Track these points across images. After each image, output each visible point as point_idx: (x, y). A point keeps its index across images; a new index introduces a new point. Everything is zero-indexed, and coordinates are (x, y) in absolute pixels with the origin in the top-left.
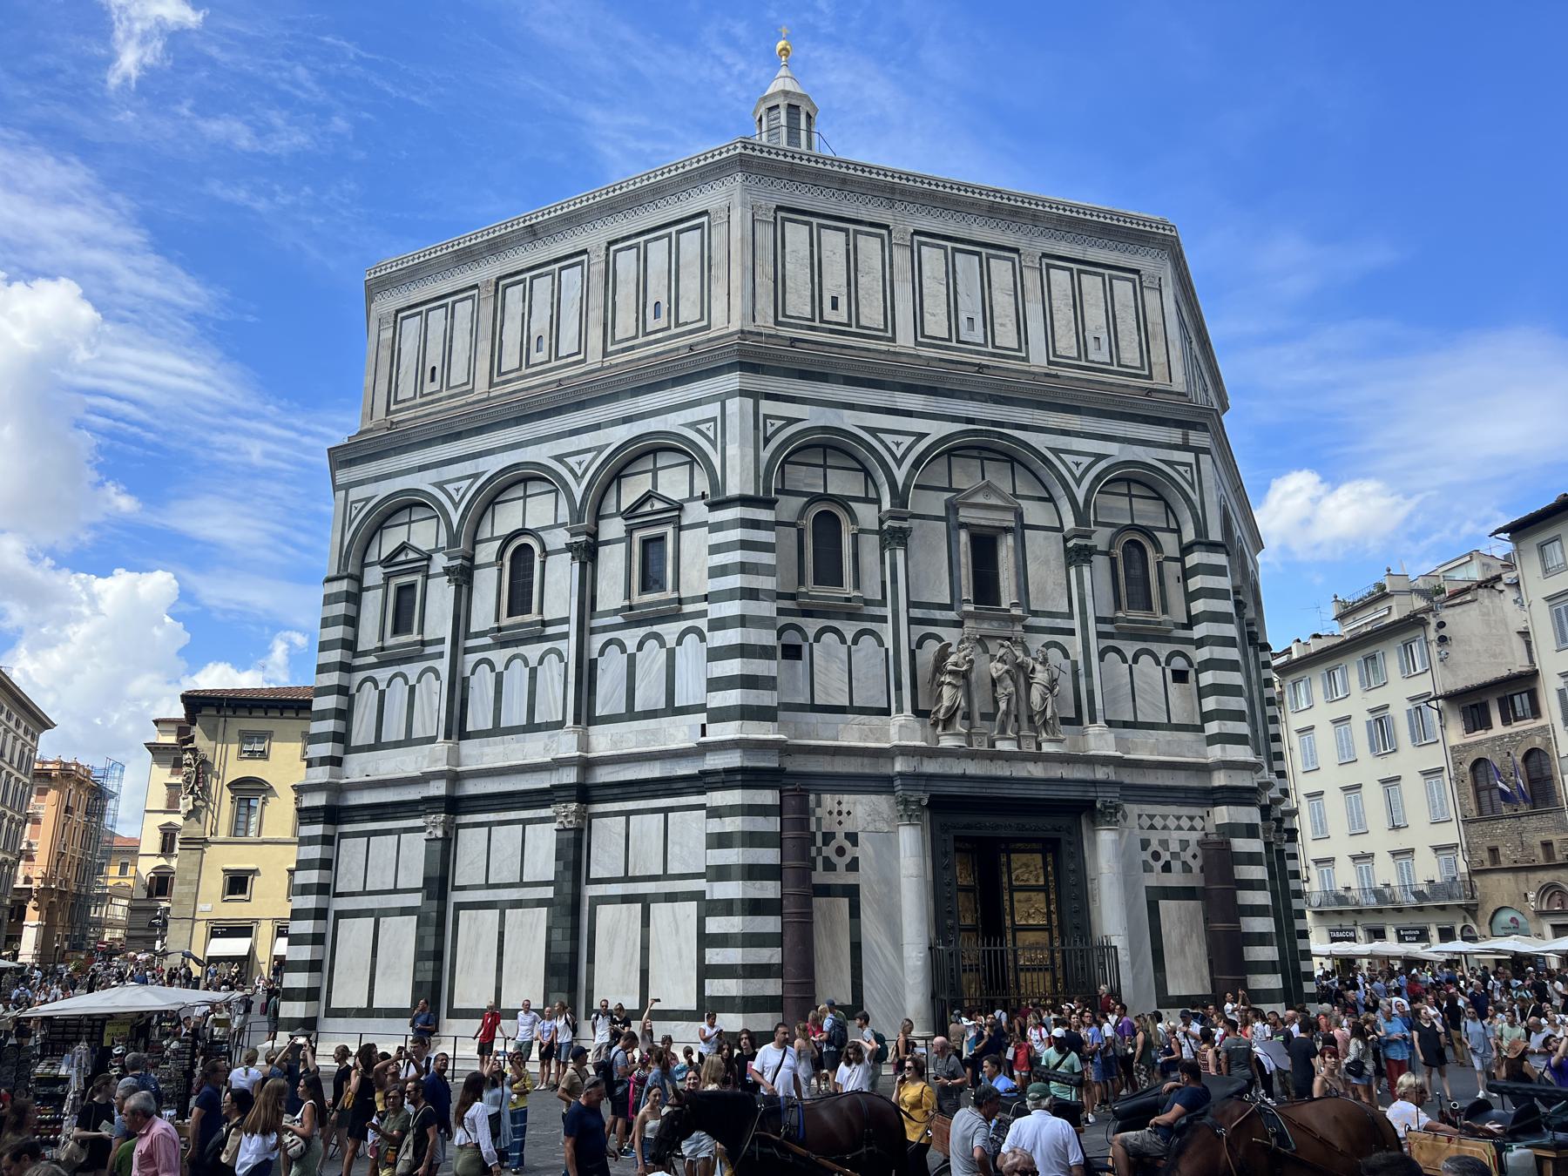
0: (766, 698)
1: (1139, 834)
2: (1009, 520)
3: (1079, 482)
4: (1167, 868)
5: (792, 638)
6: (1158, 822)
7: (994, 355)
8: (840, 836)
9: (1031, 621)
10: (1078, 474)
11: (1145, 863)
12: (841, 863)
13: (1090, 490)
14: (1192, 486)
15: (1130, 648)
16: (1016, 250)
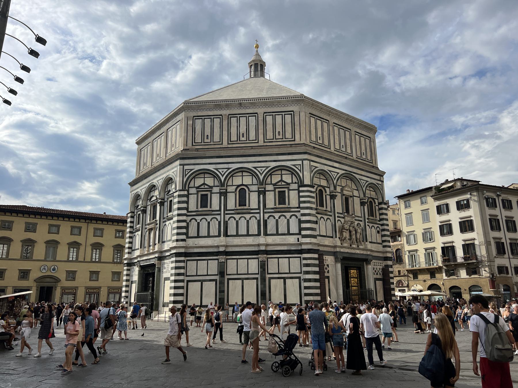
14: (176, 176)
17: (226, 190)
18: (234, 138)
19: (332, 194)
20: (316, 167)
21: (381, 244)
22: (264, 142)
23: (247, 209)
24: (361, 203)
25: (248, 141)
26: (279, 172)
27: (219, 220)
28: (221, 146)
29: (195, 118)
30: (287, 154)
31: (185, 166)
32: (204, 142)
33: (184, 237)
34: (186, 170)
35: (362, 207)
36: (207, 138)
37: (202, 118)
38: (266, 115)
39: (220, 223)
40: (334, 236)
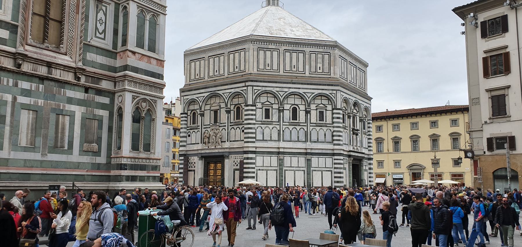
0: (184, 144)
1: (233, 160)
2: (218, 108)
3: (226, 98)
4: (237, 165)
5: (189, 134)
6: (237, 158)
7: (219, 76)
8: (193, 163)
9: (221, 125)
10: (226, 97)
11: (234, 164)
12: (193, 166)
13: (228, 100)
14: (246, 94)
15: (235, 127)
16: (224, 53)
17: (284, 107)
18: (288, 68)
19: (349, 115)
20: (343, 96)
21: (367, 149)
22: (309, 74)
23: (298, 123)
24: (360, 120)
25: (298, 72)
26: (320, 98)
27: (279, 129)
28: (278, 74)
29: (259, 49)
30: (327, 85)
31: (254, 87)
32: (266, 69)
33: (254, 140)
34: (254, 90)
35: (361, 123)
36: (268, 66)
37: (265, 50)
38: (311, 53)
39: (279, 131)
40: (349, 144)
